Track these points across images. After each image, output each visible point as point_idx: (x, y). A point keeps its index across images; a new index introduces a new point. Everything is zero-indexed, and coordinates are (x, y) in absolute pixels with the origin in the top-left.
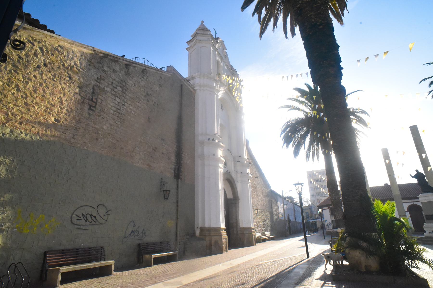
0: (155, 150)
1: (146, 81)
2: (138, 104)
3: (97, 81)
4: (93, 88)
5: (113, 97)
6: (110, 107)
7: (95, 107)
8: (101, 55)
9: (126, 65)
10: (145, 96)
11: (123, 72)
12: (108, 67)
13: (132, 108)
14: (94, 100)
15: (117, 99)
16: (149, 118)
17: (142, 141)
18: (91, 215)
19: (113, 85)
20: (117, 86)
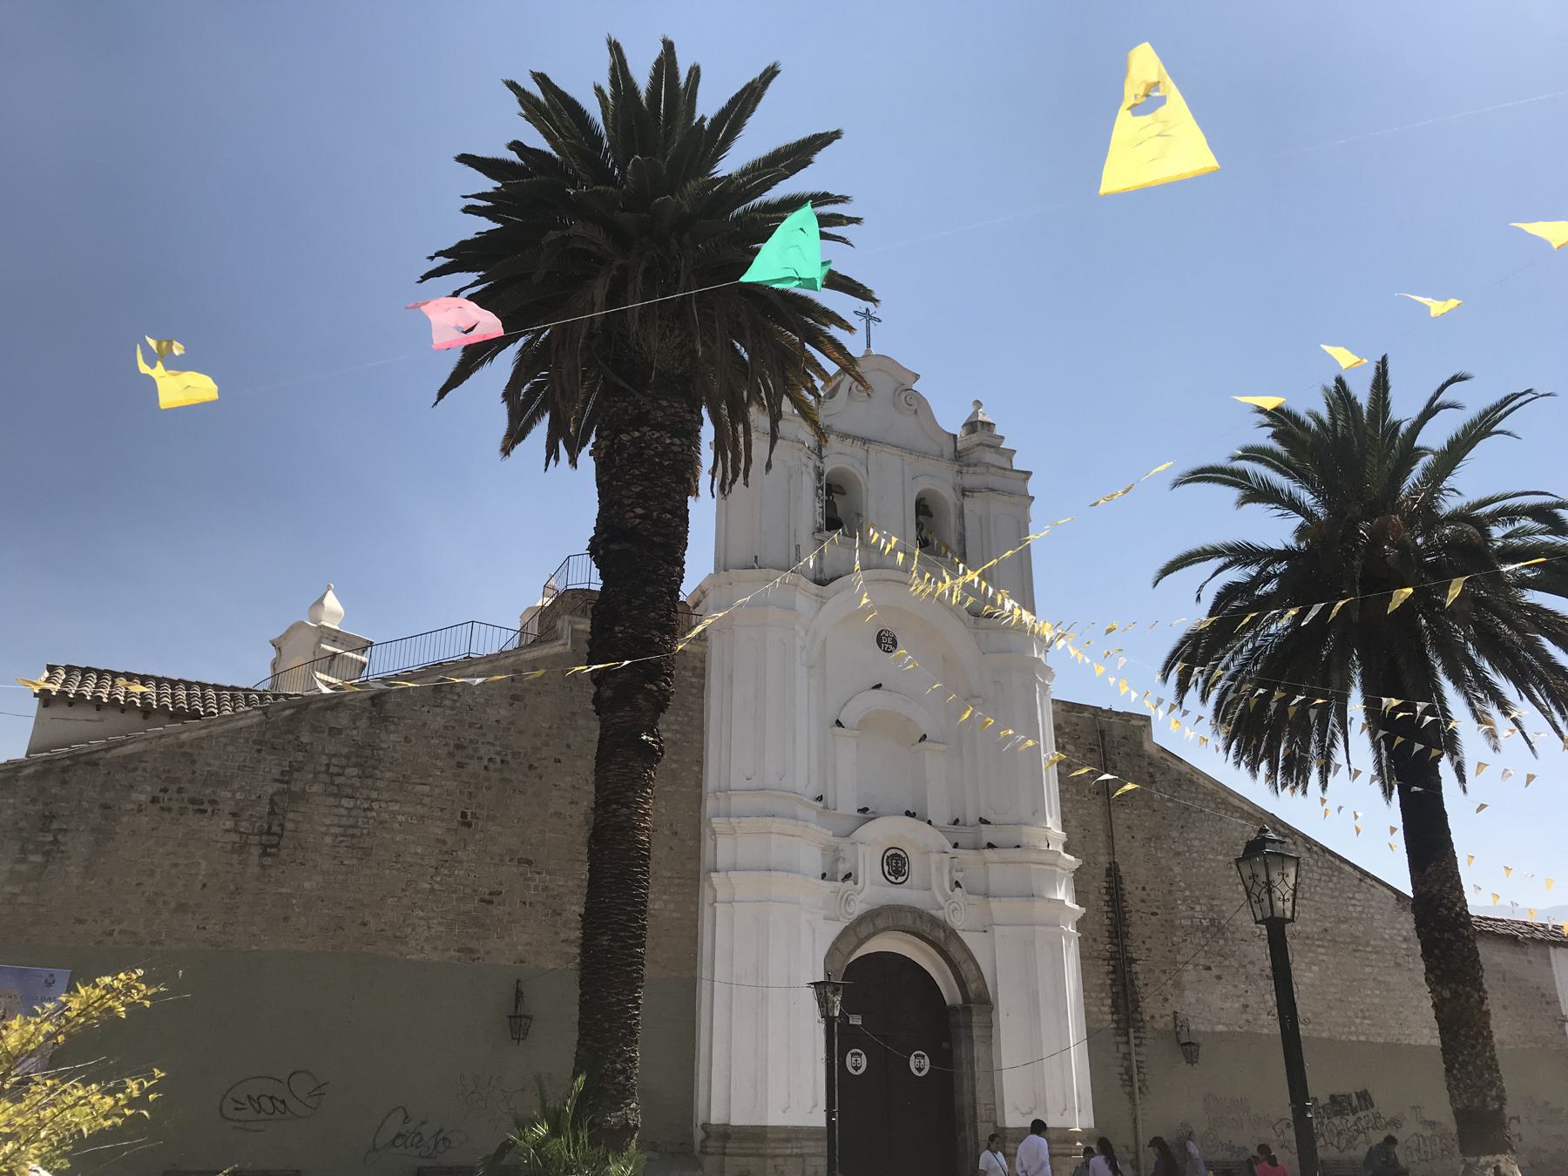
0: (491, 902)
1: (452, 709)
2: (419, 788)
3: (281, 781)
4: (272, 801)
5: (331, 801)
6: (323, 829)
7: (277, 846)
8: (288, 712)
9: (372, 698)
10: (451, 754)
11: (363, 723)
12: (314, 729)
13: (397, 807)
14: (275, 829)
15: (345, 802)
16: (464, 815)
17: (436, 886)
18: (271, 1098)
19: (333, 770)
20: (343, 767)
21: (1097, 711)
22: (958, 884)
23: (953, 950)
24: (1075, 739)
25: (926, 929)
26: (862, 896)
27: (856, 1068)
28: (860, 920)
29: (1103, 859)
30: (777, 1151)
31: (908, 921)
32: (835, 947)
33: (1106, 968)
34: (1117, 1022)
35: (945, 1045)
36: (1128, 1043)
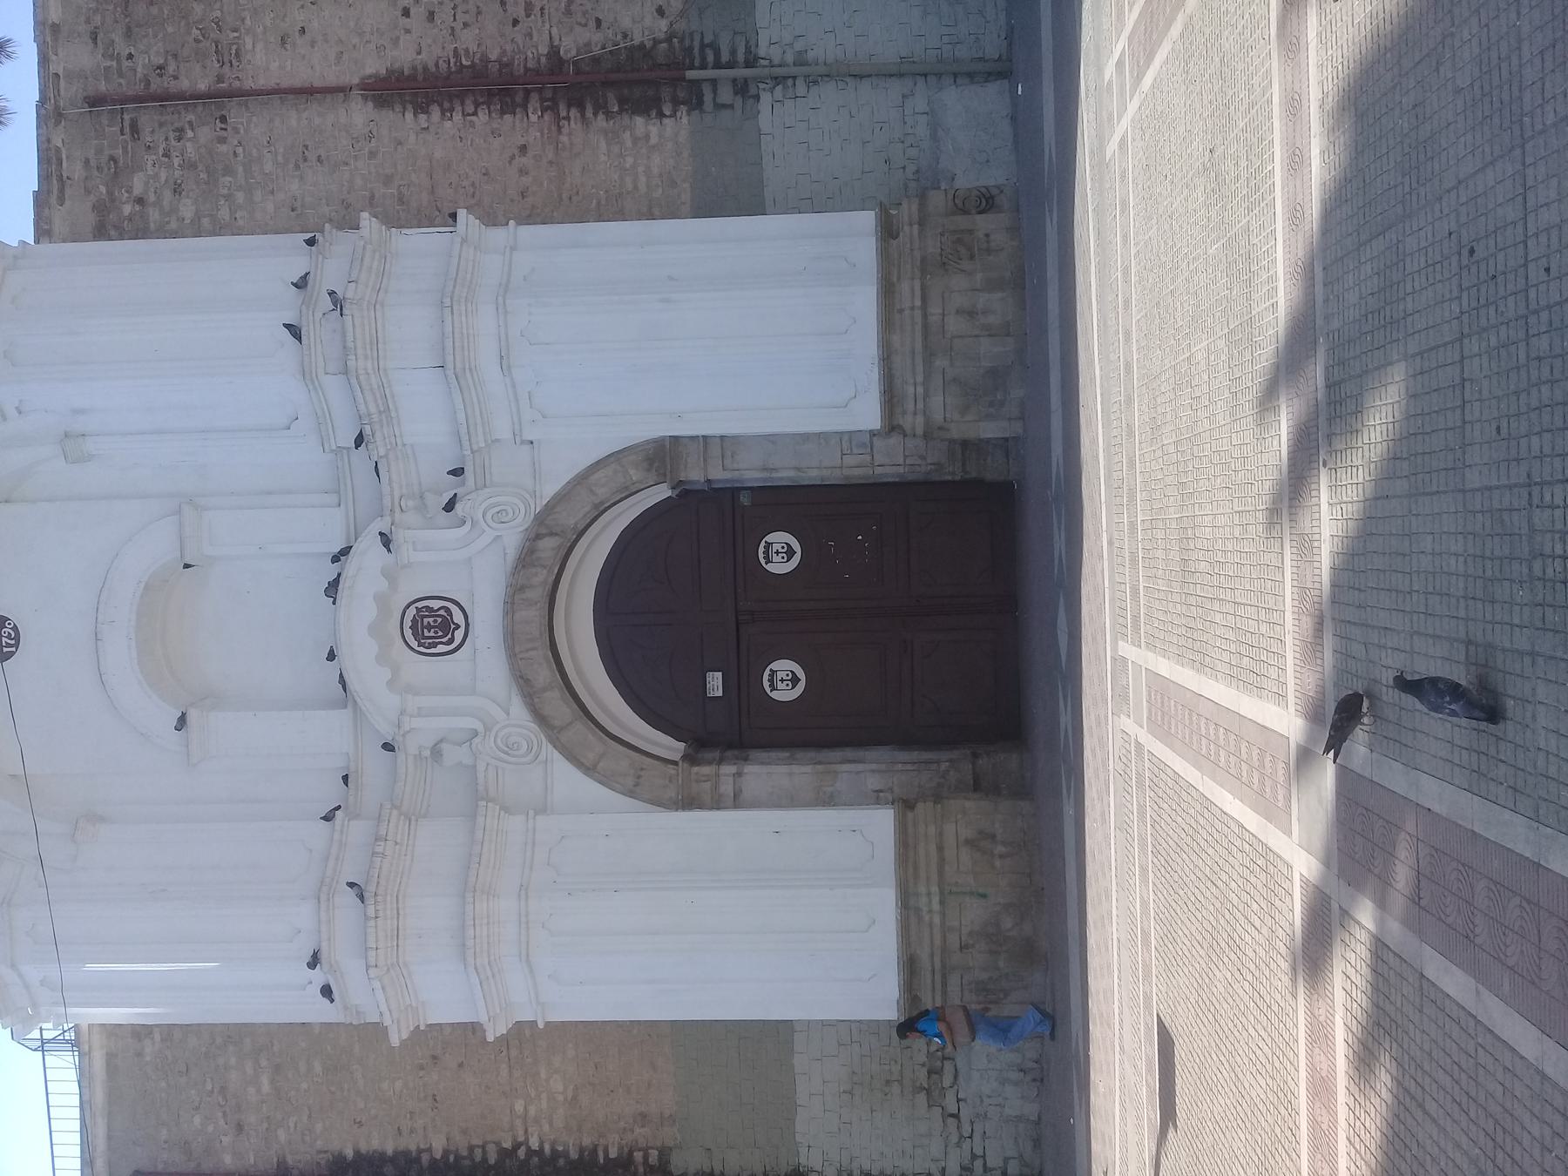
21: (50, 113)
22: (450, 506)
23: (569, 518)
24: (118, 172)
25: (542, 577)
26: (498, 713)
27: (795, 680)
28: (540, 718)
29: (359, 113)
30: (938, 942)
31: (532, 615)
32: (589, 770)
33: (575, 125)
34: (676, 103)
35: (745, 500)
36: (714, 82)
